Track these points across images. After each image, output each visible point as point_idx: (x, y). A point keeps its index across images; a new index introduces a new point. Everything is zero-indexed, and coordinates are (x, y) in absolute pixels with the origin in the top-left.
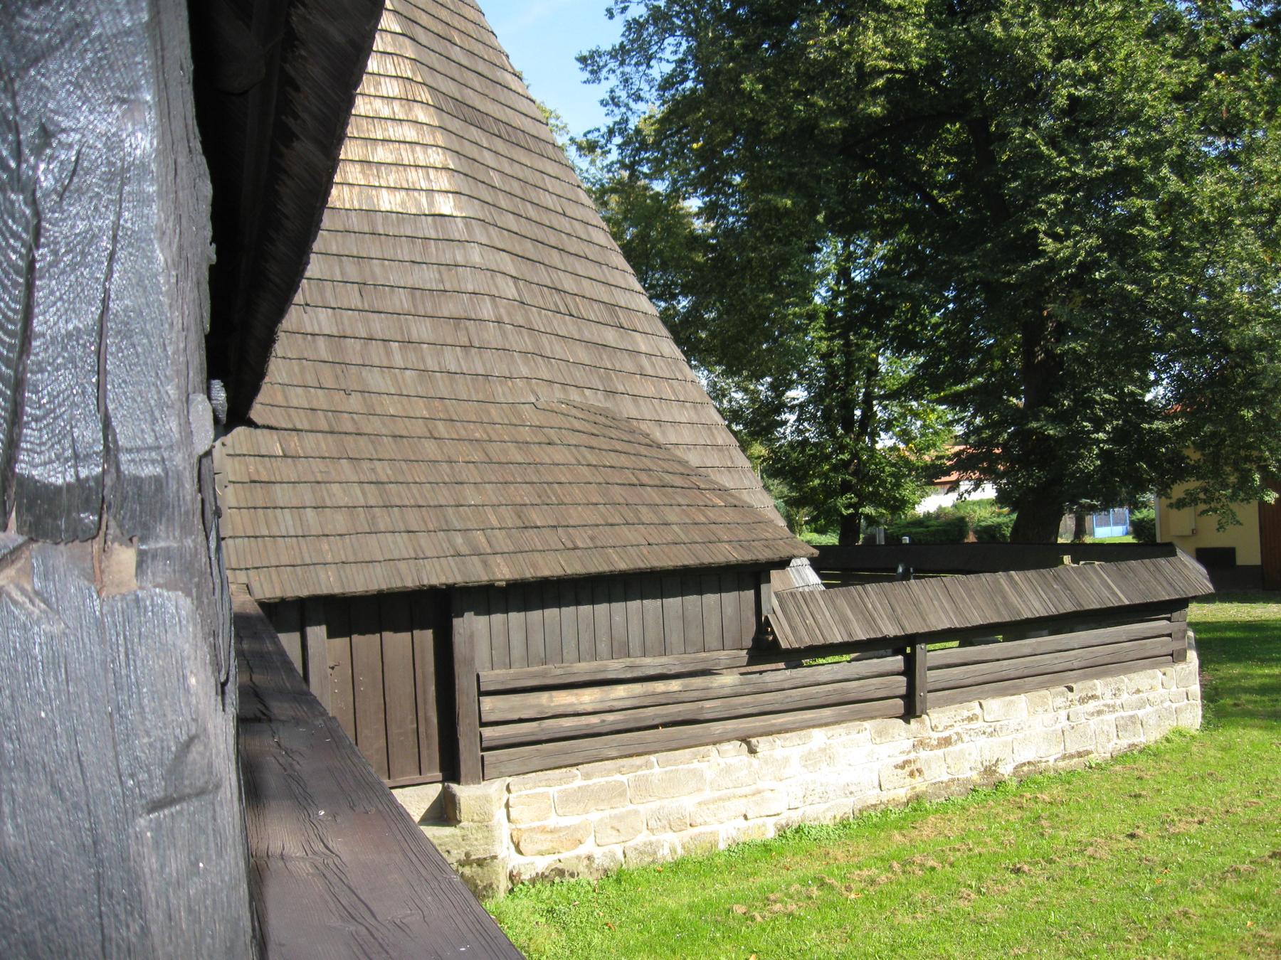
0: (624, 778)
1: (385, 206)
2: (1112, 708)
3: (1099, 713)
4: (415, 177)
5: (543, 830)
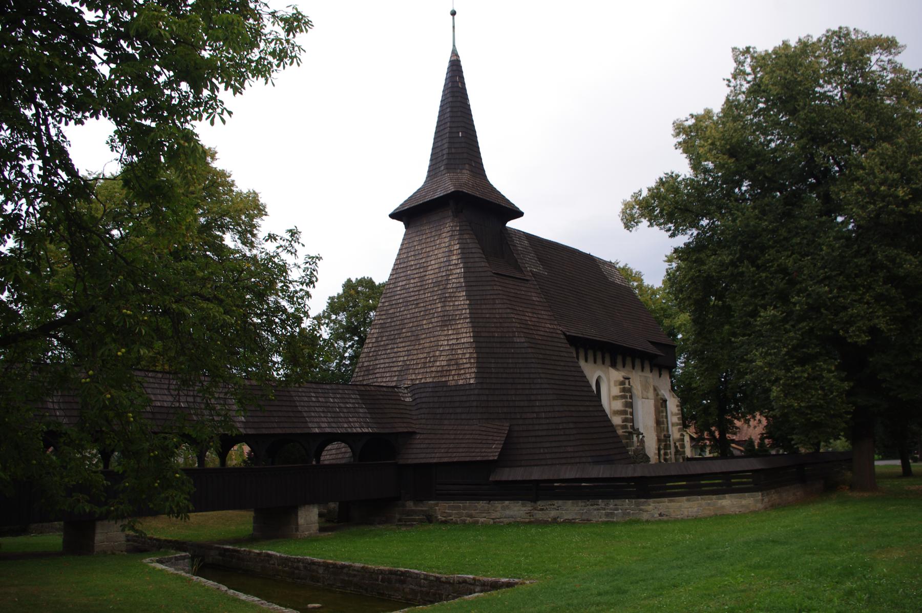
0: (461, 505)
1: (460, 383)
2: (604, 509)
3: (598, 509)
4: (468, 376)
5: (445, 512)
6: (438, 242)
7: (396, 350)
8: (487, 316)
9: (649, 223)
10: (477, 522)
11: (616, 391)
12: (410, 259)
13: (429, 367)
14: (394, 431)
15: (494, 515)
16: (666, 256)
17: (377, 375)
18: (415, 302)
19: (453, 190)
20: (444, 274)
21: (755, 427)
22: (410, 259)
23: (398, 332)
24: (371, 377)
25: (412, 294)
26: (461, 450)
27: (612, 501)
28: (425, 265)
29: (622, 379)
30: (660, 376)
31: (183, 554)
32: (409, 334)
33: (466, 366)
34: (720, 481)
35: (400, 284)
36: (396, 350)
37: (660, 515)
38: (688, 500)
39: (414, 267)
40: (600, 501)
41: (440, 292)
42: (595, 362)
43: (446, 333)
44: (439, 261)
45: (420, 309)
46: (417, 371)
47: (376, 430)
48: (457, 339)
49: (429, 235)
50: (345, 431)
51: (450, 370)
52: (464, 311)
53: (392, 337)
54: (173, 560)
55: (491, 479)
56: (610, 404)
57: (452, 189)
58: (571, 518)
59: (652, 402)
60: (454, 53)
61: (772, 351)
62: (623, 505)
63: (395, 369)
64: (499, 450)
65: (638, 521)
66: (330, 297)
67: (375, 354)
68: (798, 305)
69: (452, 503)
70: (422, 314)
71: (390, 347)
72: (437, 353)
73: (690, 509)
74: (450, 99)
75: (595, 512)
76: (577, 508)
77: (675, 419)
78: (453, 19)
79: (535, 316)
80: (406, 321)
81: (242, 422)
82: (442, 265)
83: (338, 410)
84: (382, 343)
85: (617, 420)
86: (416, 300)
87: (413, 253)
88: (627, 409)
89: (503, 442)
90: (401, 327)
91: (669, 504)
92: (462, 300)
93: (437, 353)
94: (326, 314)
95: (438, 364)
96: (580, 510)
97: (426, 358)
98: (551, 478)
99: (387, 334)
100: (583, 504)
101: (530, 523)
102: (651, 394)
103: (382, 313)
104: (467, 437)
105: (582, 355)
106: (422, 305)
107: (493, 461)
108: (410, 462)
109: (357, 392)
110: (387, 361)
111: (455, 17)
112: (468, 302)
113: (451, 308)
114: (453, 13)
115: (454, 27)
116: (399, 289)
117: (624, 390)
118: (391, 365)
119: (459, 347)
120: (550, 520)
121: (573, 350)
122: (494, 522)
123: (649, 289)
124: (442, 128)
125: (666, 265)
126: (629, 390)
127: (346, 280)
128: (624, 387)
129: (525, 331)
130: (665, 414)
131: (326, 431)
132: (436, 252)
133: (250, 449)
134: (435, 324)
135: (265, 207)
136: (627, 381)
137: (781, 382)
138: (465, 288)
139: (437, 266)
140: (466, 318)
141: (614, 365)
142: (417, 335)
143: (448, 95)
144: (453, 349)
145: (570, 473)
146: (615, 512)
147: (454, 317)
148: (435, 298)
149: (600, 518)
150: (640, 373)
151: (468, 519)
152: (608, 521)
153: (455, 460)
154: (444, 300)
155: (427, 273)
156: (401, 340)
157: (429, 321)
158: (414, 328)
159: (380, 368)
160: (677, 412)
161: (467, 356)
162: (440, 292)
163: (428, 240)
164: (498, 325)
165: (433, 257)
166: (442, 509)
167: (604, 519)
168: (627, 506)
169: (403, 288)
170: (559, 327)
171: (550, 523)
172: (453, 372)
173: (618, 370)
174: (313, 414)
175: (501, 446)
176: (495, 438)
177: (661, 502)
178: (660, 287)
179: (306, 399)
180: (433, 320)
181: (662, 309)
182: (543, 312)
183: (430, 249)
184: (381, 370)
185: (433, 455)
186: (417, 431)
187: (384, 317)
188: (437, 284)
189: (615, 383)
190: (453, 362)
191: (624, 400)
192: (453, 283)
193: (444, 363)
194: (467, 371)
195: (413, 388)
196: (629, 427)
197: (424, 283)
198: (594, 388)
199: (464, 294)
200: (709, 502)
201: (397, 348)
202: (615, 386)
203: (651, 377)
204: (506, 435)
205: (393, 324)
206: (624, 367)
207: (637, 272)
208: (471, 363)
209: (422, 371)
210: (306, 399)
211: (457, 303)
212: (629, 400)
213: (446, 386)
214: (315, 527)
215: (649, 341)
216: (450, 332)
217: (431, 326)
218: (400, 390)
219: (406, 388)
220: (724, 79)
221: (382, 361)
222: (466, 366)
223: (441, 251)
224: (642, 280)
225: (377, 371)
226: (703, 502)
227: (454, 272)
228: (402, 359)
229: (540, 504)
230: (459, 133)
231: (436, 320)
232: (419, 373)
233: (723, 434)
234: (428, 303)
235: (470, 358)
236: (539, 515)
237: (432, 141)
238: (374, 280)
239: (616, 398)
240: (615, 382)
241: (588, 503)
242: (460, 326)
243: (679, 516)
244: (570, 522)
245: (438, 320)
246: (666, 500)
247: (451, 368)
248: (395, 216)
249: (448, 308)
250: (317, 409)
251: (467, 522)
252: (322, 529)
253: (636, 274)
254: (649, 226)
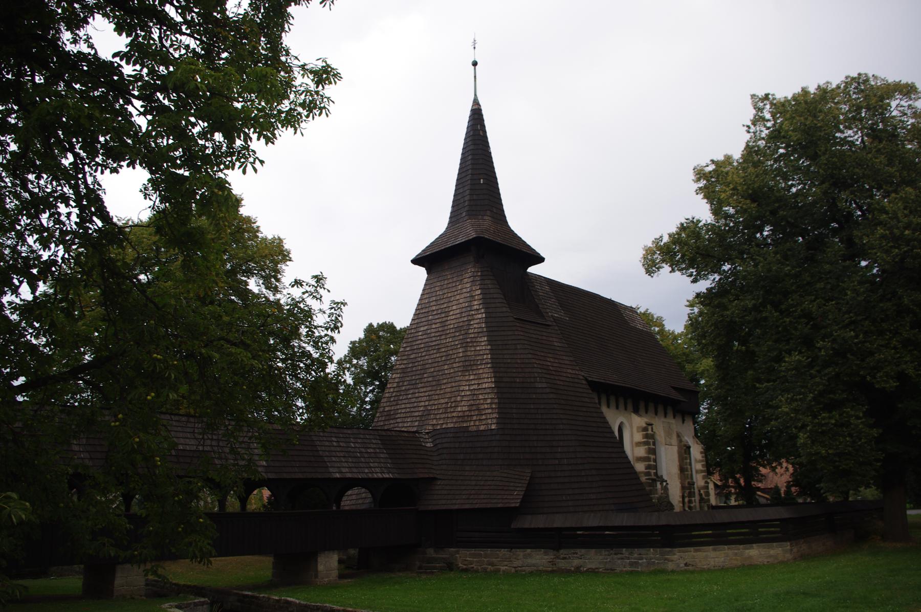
1: (481, 429)
2: (628, 558)
4: (489, 421)
5: (466, 560)
6: (460, 287)
7: (417, 395)
8: (509, 361)
9: (670, 269)
10: (499, 570)
11: (638, 437)
12: (432, 304)
13: (451, 412)
14: (415, 476)
15: (517, 563)
16: (688, 301)
17: (399, 420)
18: (437, 347)
19: (475, 236)
20: (465, 319)
21: (781, 475)
22: (432, 304)
23: (420, 377)
24: (392, 422)
25: (434, 339)
26: (482, 496)
27: (636, 550)
28: (446, 310)
29: (644, 425)
30: (683, 422)
31: (202, 600)
32: (430, 379)
33: (487, 411)
34: (747, 530)
35: (422, 329)
36: (417, 395)
37: (686, 565)
38: (715, 550)
39: (435, 313)
40: (624, 549)
41: (461, 337)
42: (617, 408)
43: (467, 378)
44: (460, 306)
45: (442, 354)
46: (438, 417)
47: (397, 476)
48: (479, 384)
49: (451, 281)
50: (366, 477)
51: (471, 415)
52: (485, 357)
53: (414, 382)
54: (192, 606)
55: (512, 527)
56: (633, 450)
57: (473, 235)
58: (594, 567)
59: (675, 449)
60: (476, 102)
61: (798, 397)
62: (647, 554)
63: (416, 414)
64: (521, 497)
65: (663, 571)
66: (351, 342)
67: (396, 398)
68: (823, 350)
69: (473, 551)
70: (443, 358)
71: (411, 391)
72: (459, 398)
73: (716, 559)
74: (472, 147)
75: (619, 561)
76: (601, 557)
77: (699, 466)
78: (475, 69)
79: (557, 361)
80: (427, 366)
81: (263, 466)
82: (464, 310)
83: (359, 455)
84: (404, 388)
85: (640, 467)
86: (438, 345)
87: (434, 299)
88: (650, 456)
89: (524, 489)
90: (422, 372)
91: (695, 554)
92: (483, 346)
93: (459, 398)
94: (348, 358)
95: (459, 409)
96: (604, 559)
97: (447, 403)
98: (574, 526)
99: (408, 379)
100: (607, 553)
101: (552, 572)
102: (674, 440)
103: (404, 358)
104: (489, 483)
105: (604, 401)
106: (443, 350)
107: (515, 507)
108: (430, 508)
109: (378, 438)
110: (408, 406)
111: (477, 67)
112: (489, 347)
113: (473, 353)
114: (475, 64)
115: (475, 77)
116: (420, 334)
117: (647, 436)
118: (412, 410)
119: (480, 392)
120: (573, 569)
121: (595, 396)
122: (516, 571)
123: (670, 334)
124: (463, 175)
125: (688, 310)
126: (652, 436)
127: (367, 325)
128: (647, 434)
129: (546, 376)
130: (688, 461)
131: (347, 477)
132: (458, 297)
133: (270, 493)
134: (456, 369)
135: (289, 253)
136: (650, 428)
137: (808, 428)
138: (486, 334)
139: (458, 311)
140: (488, 363)
141: (636, 411)
142: (438, 380)
143: (470, 143)
144: (474, 394)
145: (592, 521)
146: (640, 561)
147: (475, 362)
148: (457, 343)
149: (625, 567)
150: (663, 419)
151: (490, 567)
152: (633, 571)
153: (477, 506)
154: (465, 345)
155: (449, 318)
156: (422, 385)
158: (435, 373)
159: (401, 413)
160: (701, 459)
161: (489, 401)
162: (461, 337)
163: (450, 285)
164: (520, 370)
165: (454, 303)
166: (464, 556)
167: (628, 569)
168: (652, 556)
169: (425, 333)
170: (580, 373)
171: (573, 572)
172: (475, 418)
173: (640, 416)
174: (334, 459)
175: (523, 493)
176: (517, 485)
177: (687, 552)
178: (682, 332)
179: (327, 444)
180: (455, 365)
181: (684, 354)
182: (564, 358)
183: (452, 294)
184: (402, 415)
185: (454, 501)
186: (438, 477)
187: (405, 362)
188: (459, 329)
189: (637, 430)
190: (474, 408)
191: (647, 447)
192: (475, 328)
193: (465, 408)
194: (488, 417)
195: (435, 434)
196: (652, 474)
197: (446, 328)
198: (617, 434)
199: (486, 339)
200: (736, 551)
201: (418, 393)
202: (638, 432)
203: (675, 424)
204: (527, 482)
205: (414, 369)
206: (646, 412)
207: (658, 317)
208: (492, 408)
209: (443, 416)
210: (327, 444)
211: (478, 348)
212: (652, 447)
213: (468, 432)
214: (335, 574)
215: (672, 387)
216: (472, 377)
218: (421, 435)
219: (427, 433)
220: (744, 126)
221: (403, 406)
222: (487, 411)
223: (463, 296)
224: (664, 325)
225: (398, 416)
226: (730, 552)
227: (476, 317)
228: (423, 404)
229: (563, 552)
230: (480, 179)
231: (457, 365)
232: (440, 418)
233: (748, 481)
234: (449, 348)
235: (491, 403)
236: (562, 564)
237: (454, 188)
238: (395, 325)
239: (638, 444)
240: (638, 428)
241: (611, 552)
242: (481, 371)
243: (705, 567)
244: (593, 572)
245: (460, 365)
246: (692, 549)
247: (473, 414)
248: (416, 261)
249: (469, 353)
250: (338, 454)
251: (488, 570)
252: (341, 576)
253: (657, 319)
254: (671, 272)
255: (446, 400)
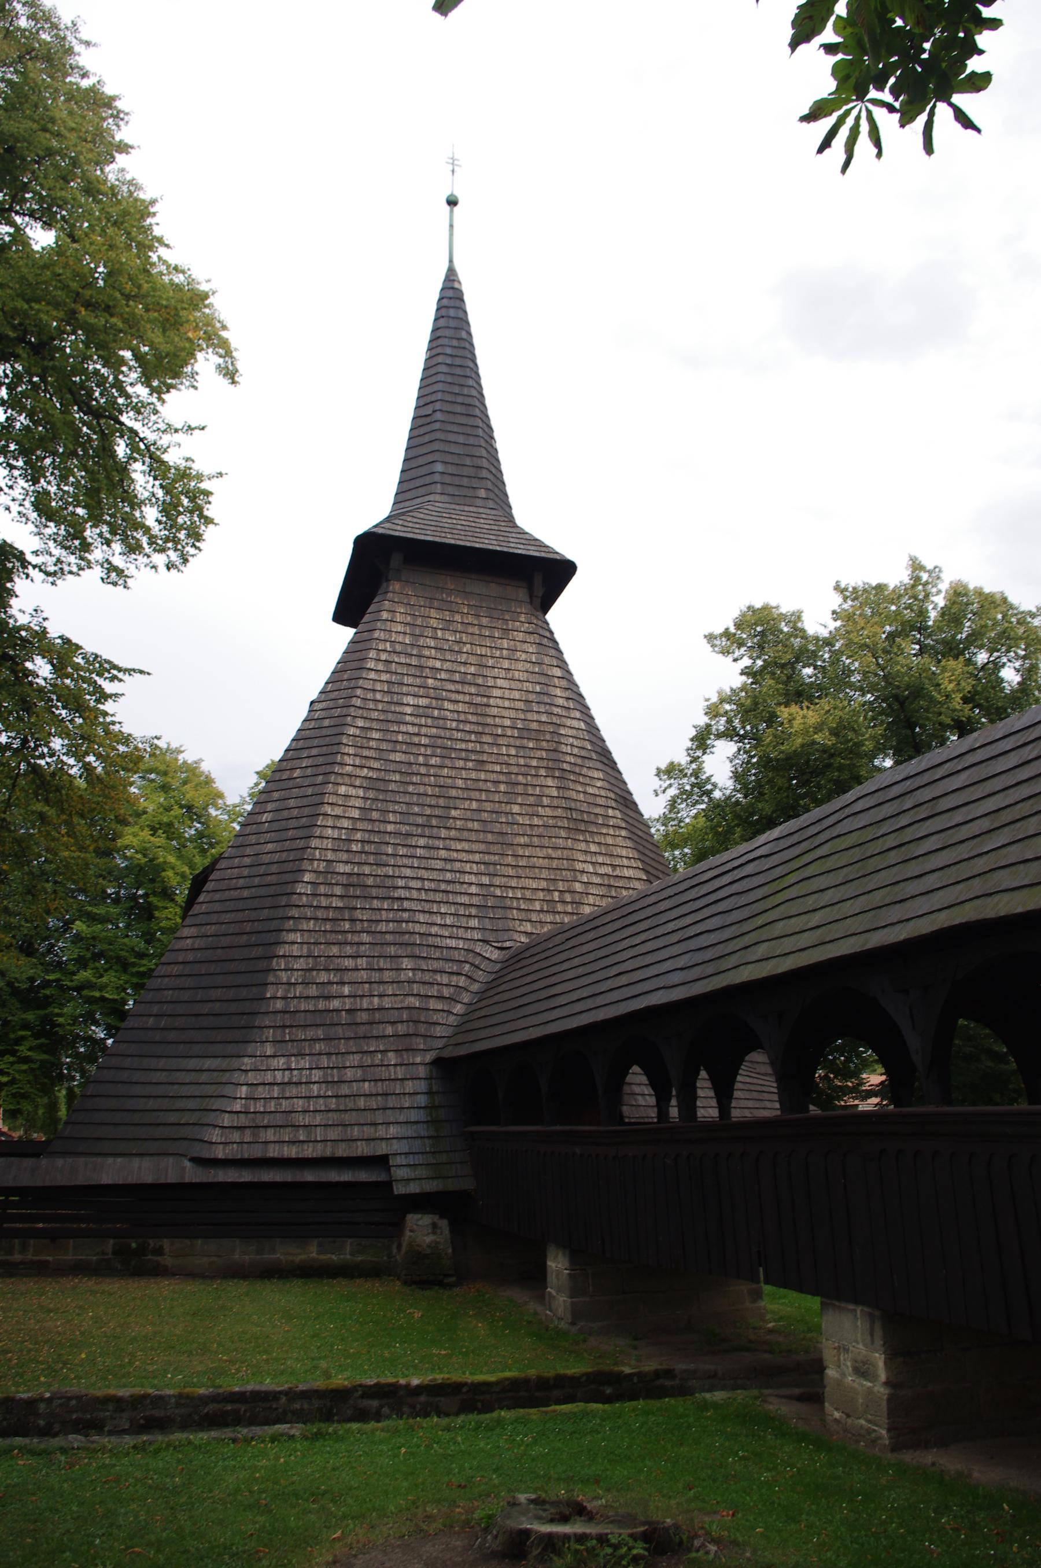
43: (583, 846)
78: (452, 212)
93: (578, 887)
103: (366, 753)
111: (456, 209)
114: (452, 202)
115: (451, 226)
155: (492, 701)
157: (530, 810)
192: (572, 745)
216: (593, 848)
217: (536, 821)
223: (520, 666)
245: (556, 814)
255: (543, 884)
